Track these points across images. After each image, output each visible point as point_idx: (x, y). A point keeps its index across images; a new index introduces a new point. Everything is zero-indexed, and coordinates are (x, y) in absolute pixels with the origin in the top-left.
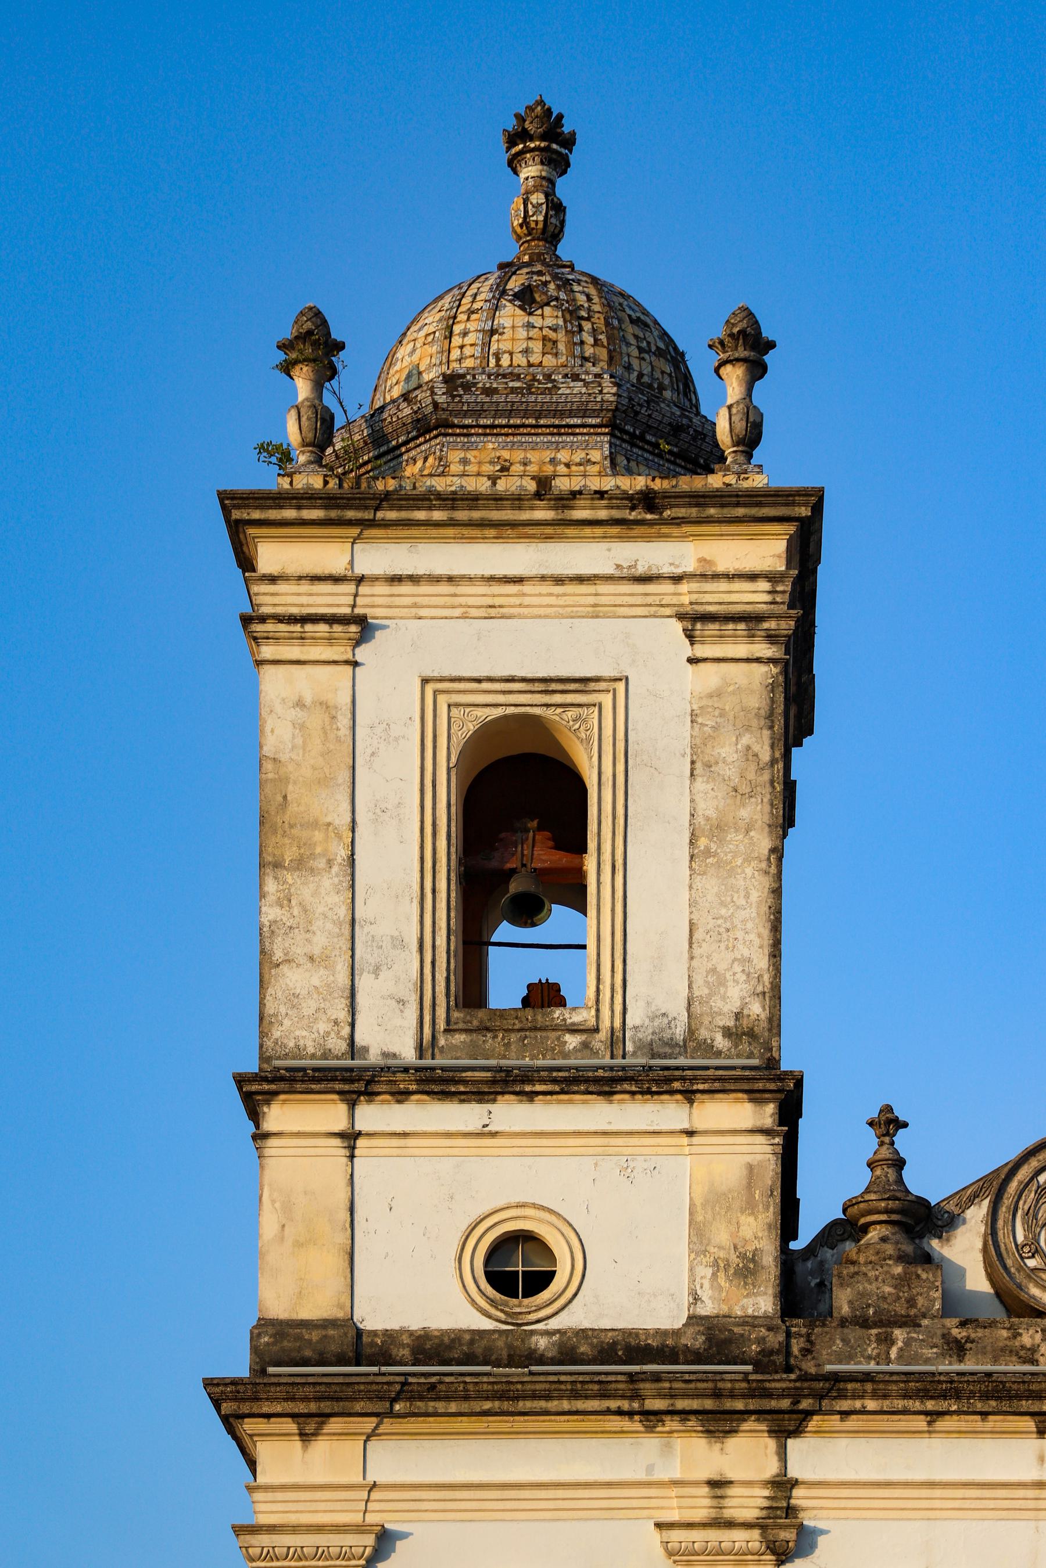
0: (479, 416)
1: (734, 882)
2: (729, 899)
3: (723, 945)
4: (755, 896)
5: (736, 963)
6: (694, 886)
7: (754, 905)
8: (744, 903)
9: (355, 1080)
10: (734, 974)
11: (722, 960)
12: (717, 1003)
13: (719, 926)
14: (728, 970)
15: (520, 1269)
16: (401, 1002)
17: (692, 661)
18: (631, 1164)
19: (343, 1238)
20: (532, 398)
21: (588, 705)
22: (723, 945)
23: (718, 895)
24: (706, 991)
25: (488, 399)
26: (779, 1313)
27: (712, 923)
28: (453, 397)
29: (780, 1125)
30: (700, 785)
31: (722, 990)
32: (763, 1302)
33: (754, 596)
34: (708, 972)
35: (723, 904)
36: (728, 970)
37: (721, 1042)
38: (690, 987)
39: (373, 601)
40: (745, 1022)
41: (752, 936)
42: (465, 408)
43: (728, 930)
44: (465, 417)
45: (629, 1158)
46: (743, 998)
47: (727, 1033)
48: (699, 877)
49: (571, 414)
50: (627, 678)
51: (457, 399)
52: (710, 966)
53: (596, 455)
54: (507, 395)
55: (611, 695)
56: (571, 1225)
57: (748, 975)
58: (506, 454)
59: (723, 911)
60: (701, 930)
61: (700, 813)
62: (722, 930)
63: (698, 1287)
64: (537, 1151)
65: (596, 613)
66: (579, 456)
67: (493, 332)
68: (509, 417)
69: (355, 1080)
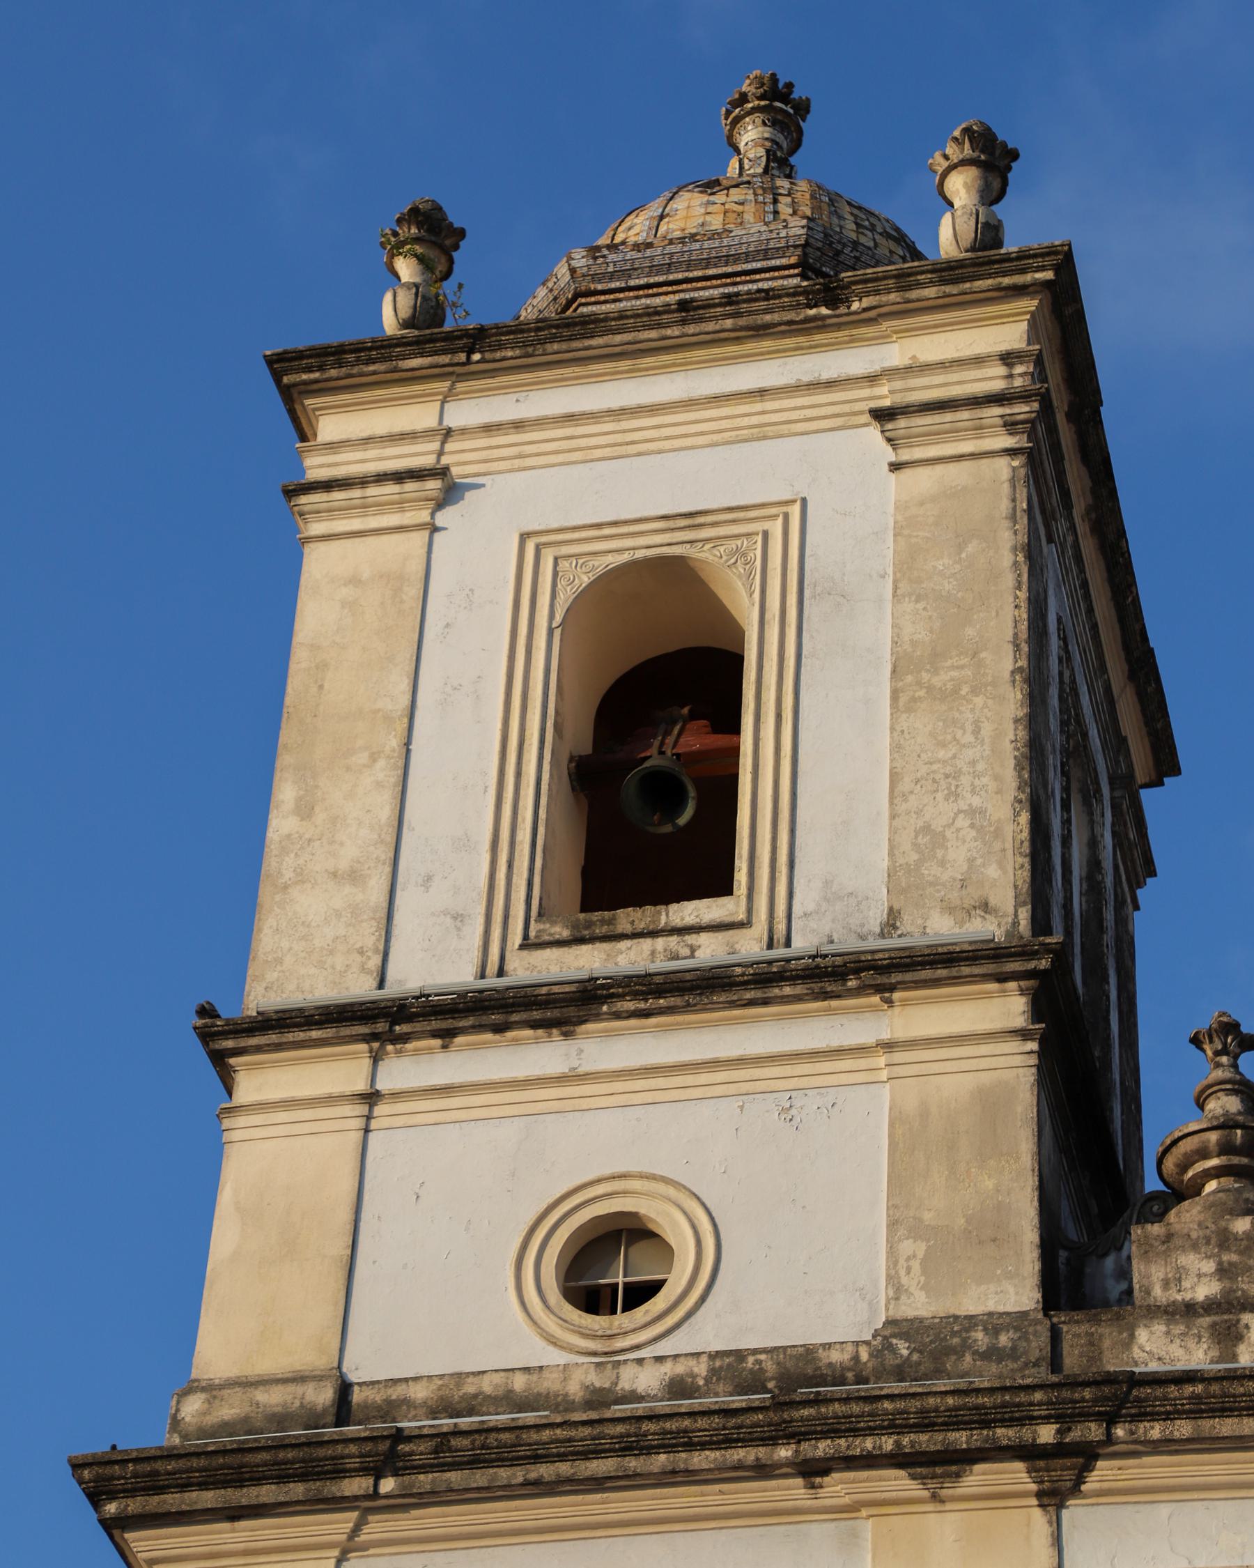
0: (630, 277)
1: (957, 715)
2: (949, 737)
3: (940, 796)
4: (987, 730)
5: (961, 816)
6: (898, 728)
7: (987, 740)
8: (972, 739)
10: (958, 830)
11: (940, 812)
12: (931, 870)
13: (934, 772)
14: (949, 826)
15: (620, 1280)
17: (895, 467)
18: (797, 1103)
19: (340, 1248)
20: (697, 246)
21: (748, 535)
22: (940, 796)
23: (932, 734)
24: (915, 856)
25: (640, 255)
26: (1041, 1306)
27: (924, 770)
28: (595, 258)
29: (1033, 1023)
31: (940, 853)
32: (1018, 1292)
33: (992, 379)
34: (917, 833)
35: (943, 745)
36: (949, 826)
38: (891, 854)
40: (973, 894)
42: (611, 269)
43: (947, 776)
44: (611, 280)
45: (794, 1094)
46: (971, 861)
47: (950, 910)
48: (905, 716)
49: (748, 257)
50: (804, 500)
51: (600, 260)
52: (920, 823)
54: (664, 247)
55: (780, 520)
56: (698, 1199)
57: (980, 830)
59: (941, 754)
60: (906, 779)
61: (906, 639)
62: (937, 777)
63: (902, 1272)
64: (649, 1097)
65: (761, 435)
67: (662, 217)
68: (669, 272)
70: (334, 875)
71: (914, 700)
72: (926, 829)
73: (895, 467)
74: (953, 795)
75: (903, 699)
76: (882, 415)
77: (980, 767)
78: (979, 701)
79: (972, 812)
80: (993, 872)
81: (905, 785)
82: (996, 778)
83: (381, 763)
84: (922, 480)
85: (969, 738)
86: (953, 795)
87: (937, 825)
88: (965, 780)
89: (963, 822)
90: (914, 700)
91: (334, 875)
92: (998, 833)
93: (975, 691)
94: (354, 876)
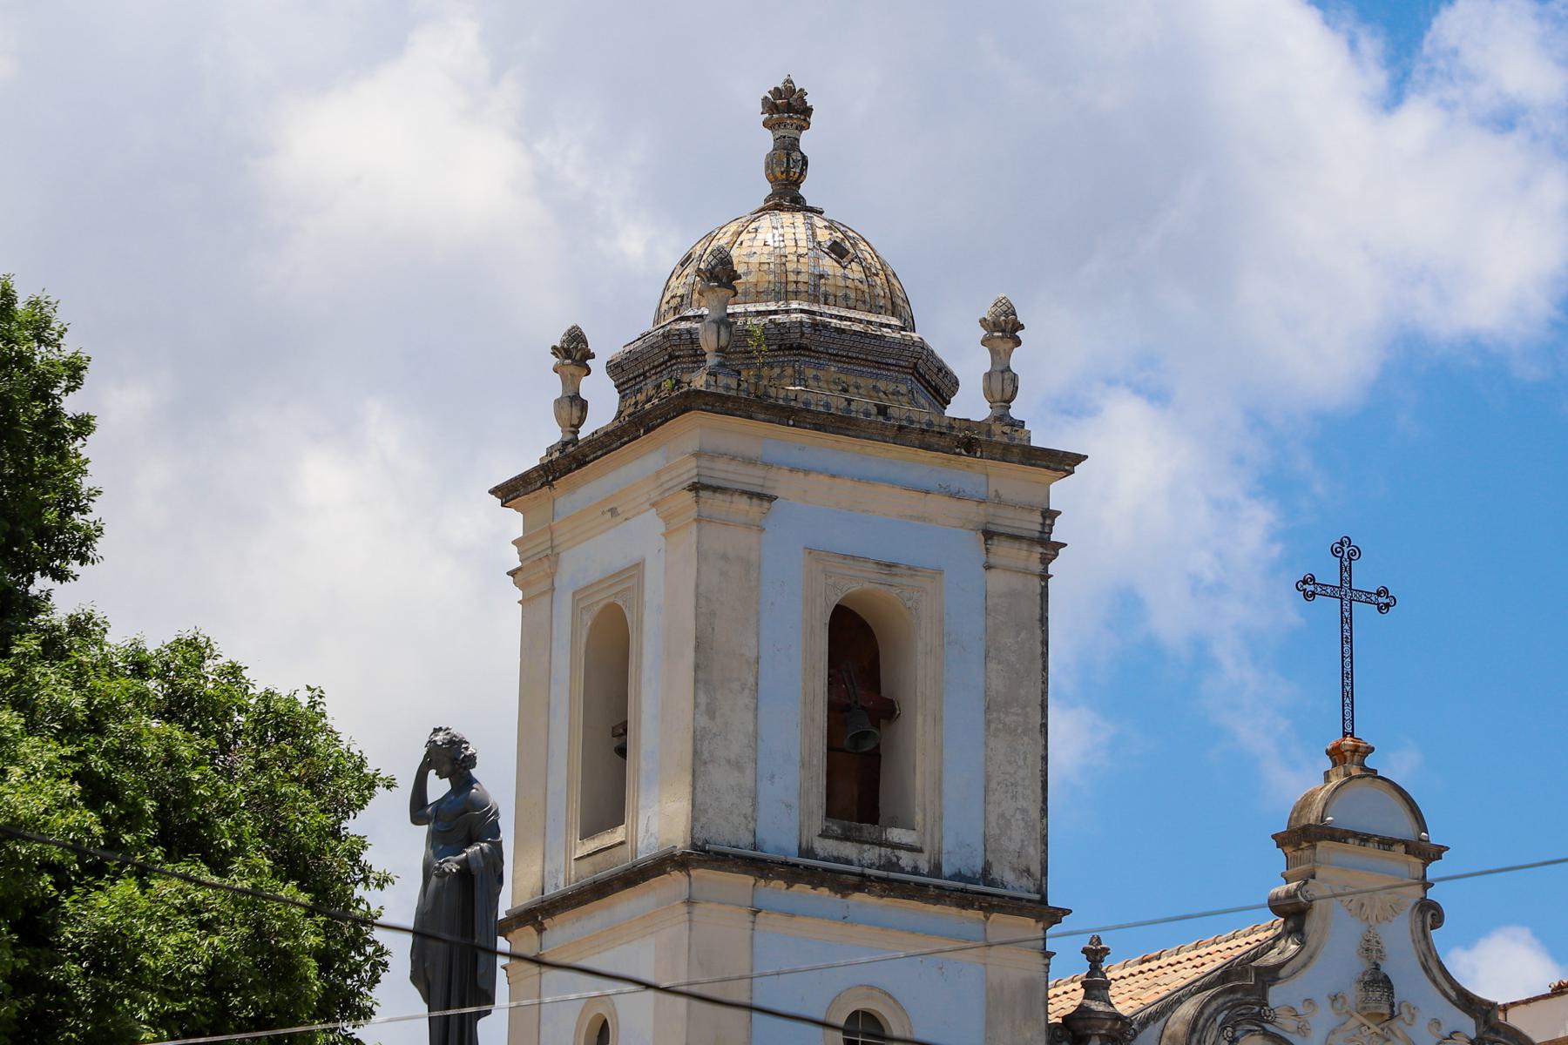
9: (757, 865)
16: (788, 806)
30: (993, 665)
37: (1009, 877)
39: (781, 483)
41: (1028, 792)
47: (1013, 869)
53: (903, 389)
58: (843, 377)
66: (891, 387)
69: (757, 865)
70: (729, 761)
71: (997, 730)
72: (1002, 815)
73: (988, 567)
74: (1014, 797)
75: (993, 727)
76: (989, 535)
77: (1027, 783)
78: (1026, 739)
79: (1024, 811)
80: (1031, 851)
81: (993, 785)
82: (1034, 792)
83: (747, 692)
84: (998, 581)
85: (1021, 763)
86: (1014, 797)
87: (1008, 815)
88: (1020, 789)
89: (1018, 816)
90: (997, 730)
91: (729, 761)
92: (1034, 828)
93: (1024, 733)
94: (737, 765)
